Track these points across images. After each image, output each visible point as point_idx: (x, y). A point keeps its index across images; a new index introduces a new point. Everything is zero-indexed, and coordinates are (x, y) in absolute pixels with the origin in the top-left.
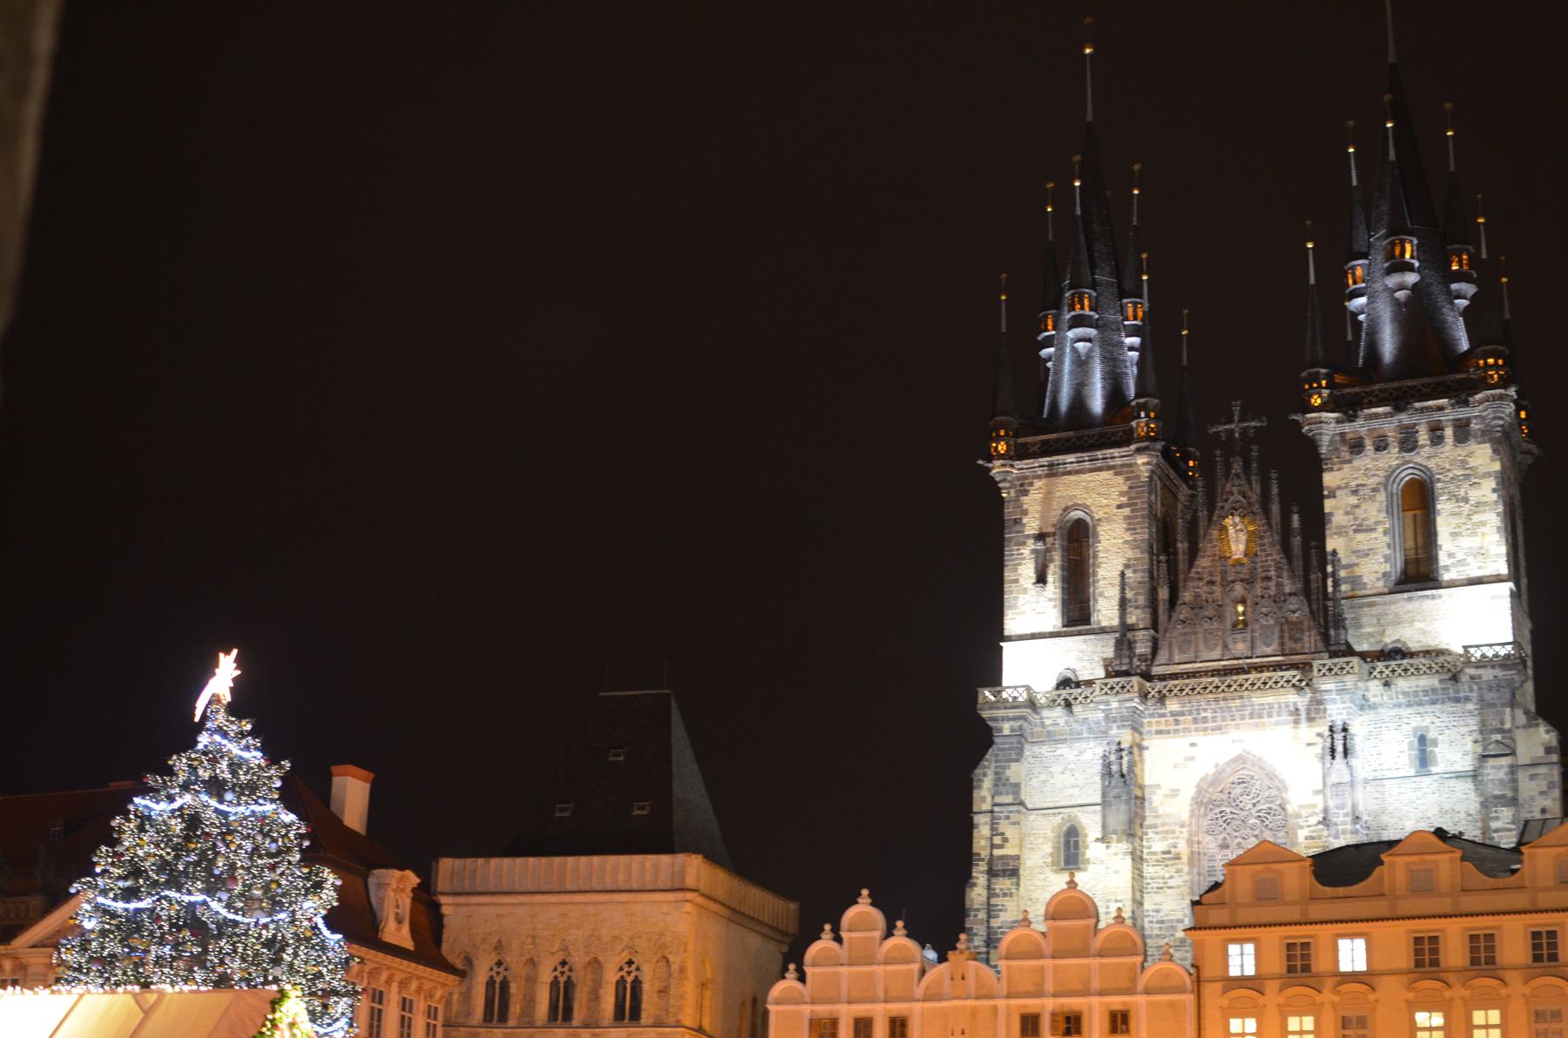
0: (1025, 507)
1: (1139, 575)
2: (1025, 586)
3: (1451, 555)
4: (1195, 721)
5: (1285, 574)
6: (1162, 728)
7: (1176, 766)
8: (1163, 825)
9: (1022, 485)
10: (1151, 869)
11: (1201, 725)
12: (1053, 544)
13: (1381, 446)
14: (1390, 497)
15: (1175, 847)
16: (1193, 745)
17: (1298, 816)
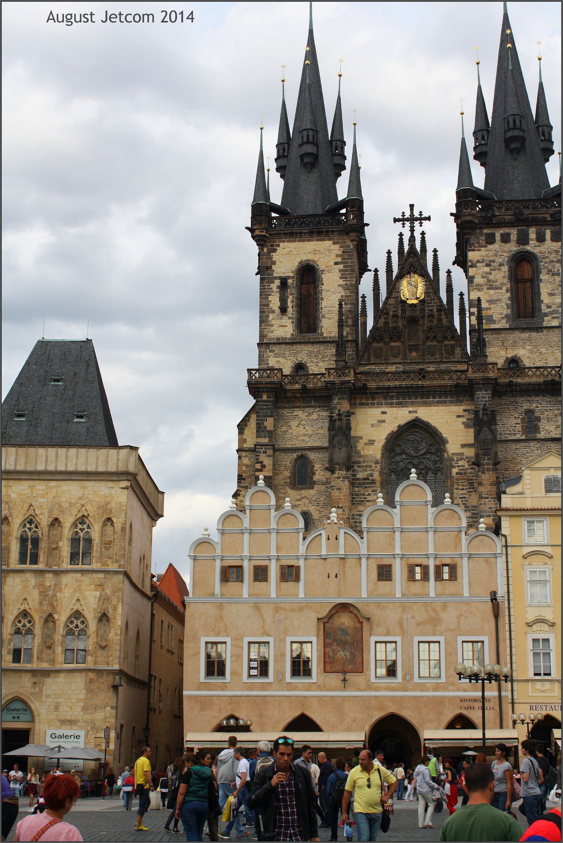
0: (274, 260)
1: (349, 306)
2: (273, 309)
3: (549, 307)
4: (385, 398)
5: (443, 313)
6: (364, 401)
7: (372, 425)
8: (364, 462)
10: (356, 489)
12: (292, 284)
13: (505, 239)
14: (510, 270)
15: (372, 476)
16: (384, 413)
17: (451, 459)
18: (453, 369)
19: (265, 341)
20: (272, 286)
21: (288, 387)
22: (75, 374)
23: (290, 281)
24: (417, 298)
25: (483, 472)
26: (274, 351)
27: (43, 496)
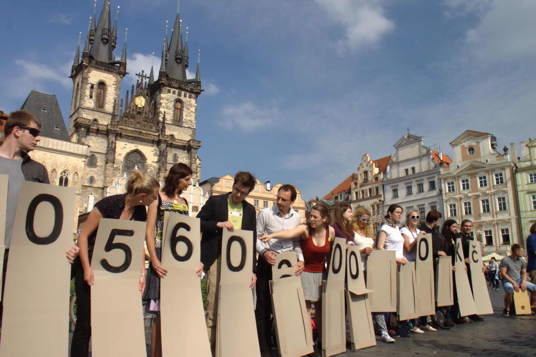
3: (185, 120)
4: (127, 139)
5: (150, 113)
7: (121, 148)
9: (89, 70)
11: (128, 140)
13: (174, 93)
15: (119, 167)
16: (126, 145)
18: (152, 134)
19: (82, 107)
20: (87, 86)
21: (91, 127)
22: (52, 109)
23: (95, 86)
24: (141, 105)
25: (161, 173)
26: (85, 112)
27: (50, 159)
